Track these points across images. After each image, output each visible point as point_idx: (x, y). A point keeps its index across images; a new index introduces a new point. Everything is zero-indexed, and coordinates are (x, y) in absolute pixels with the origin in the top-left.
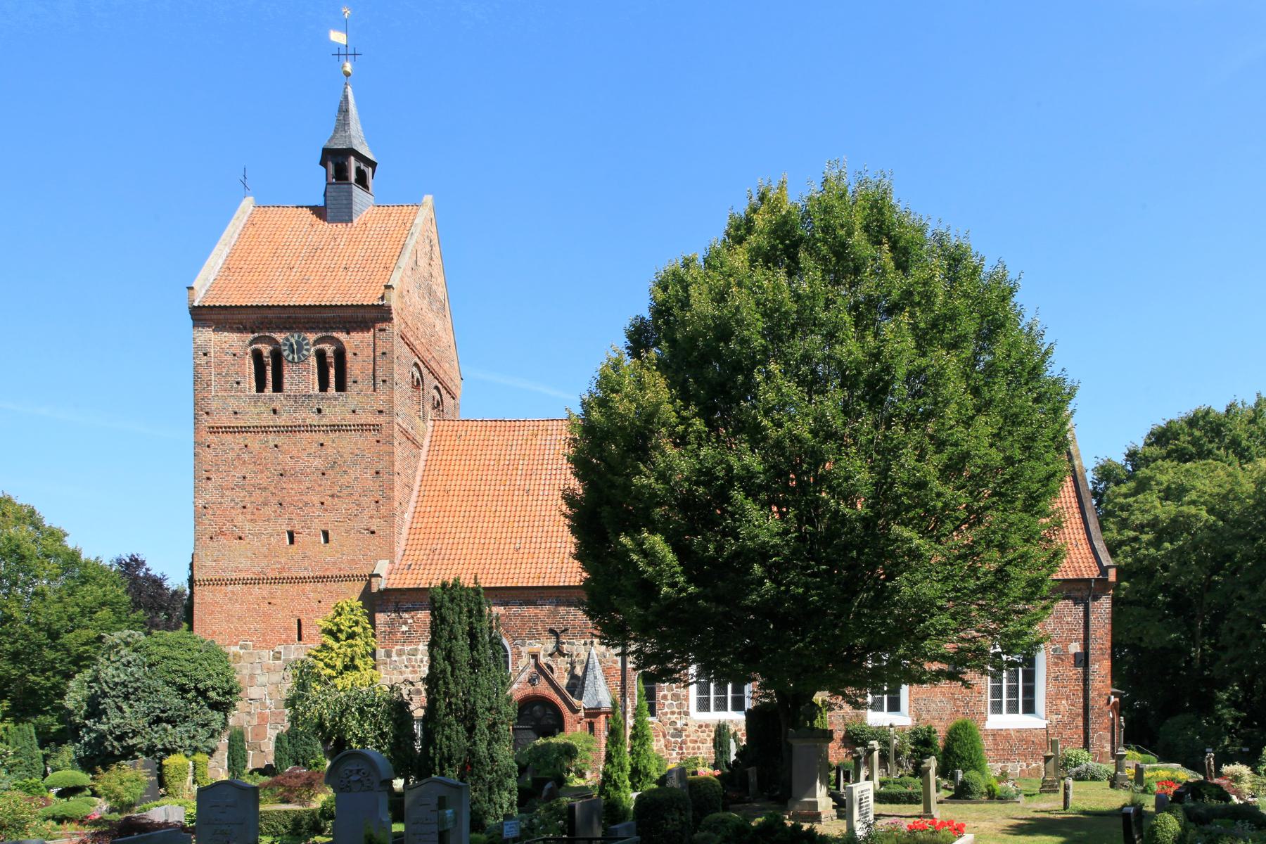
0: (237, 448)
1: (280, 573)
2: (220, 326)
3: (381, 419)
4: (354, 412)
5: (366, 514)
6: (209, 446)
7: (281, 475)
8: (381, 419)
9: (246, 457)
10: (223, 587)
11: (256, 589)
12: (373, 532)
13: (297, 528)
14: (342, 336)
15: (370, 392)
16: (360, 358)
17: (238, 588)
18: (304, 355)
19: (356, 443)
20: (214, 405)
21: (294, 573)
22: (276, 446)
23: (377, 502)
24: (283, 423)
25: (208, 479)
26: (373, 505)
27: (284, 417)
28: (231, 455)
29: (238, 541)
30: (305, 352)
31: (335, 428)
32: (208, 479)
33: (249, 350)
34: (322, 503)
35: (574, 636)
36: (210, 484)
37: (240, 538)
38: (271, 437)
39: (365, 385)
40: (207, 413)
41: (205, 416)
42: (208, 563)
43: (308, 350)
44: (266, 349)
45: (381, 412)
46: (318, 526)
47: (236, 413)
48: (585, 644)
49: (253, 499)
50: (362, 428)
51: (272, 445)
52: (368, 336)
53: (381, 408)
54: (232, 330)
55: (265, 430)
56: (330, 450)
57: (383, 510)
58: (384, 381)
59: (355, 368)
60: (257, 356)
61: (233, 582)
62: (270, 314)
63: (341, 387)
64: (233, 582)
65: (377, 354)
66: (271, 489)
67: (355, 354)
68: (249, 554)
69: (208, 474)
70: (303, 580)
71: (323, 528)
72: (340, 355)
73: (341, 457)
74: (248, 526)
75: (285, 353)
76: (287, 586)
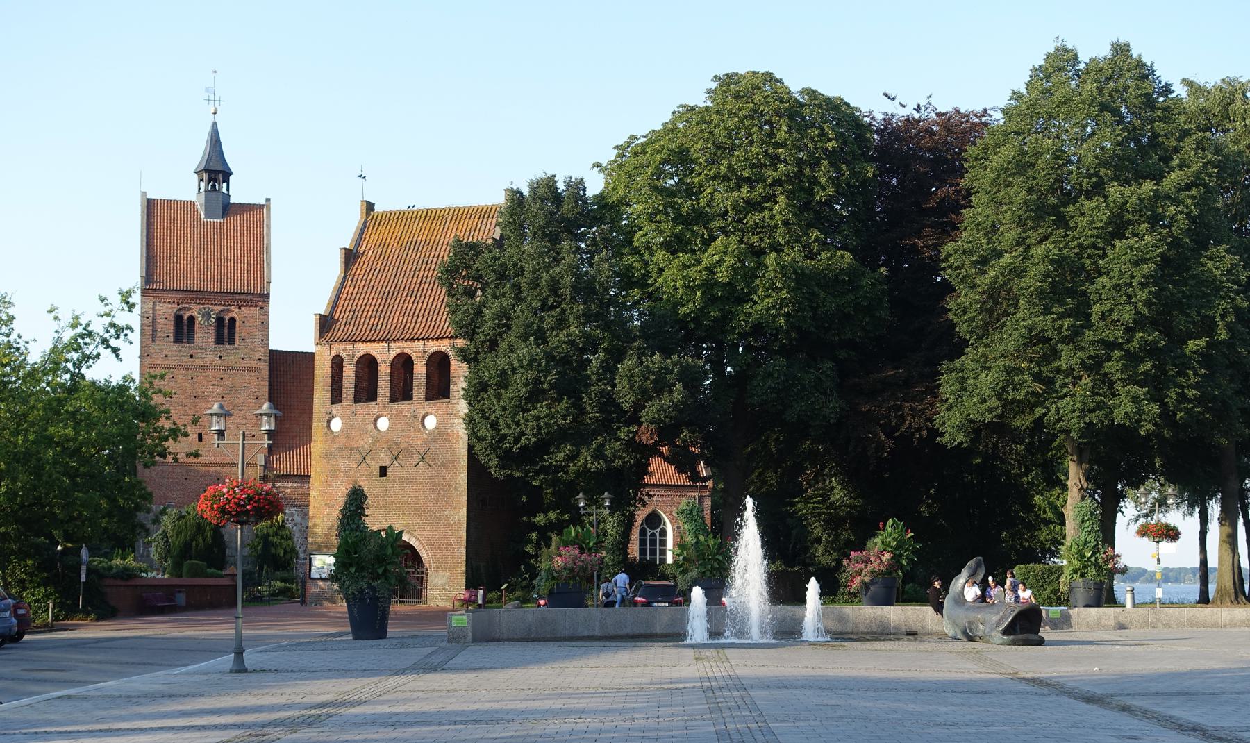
16: (247, 325)
45: (260, 359)
51: (190, 377)
55: (186, 368)
59: (240, 331)
60: (178, 319)
63: (232, 340)
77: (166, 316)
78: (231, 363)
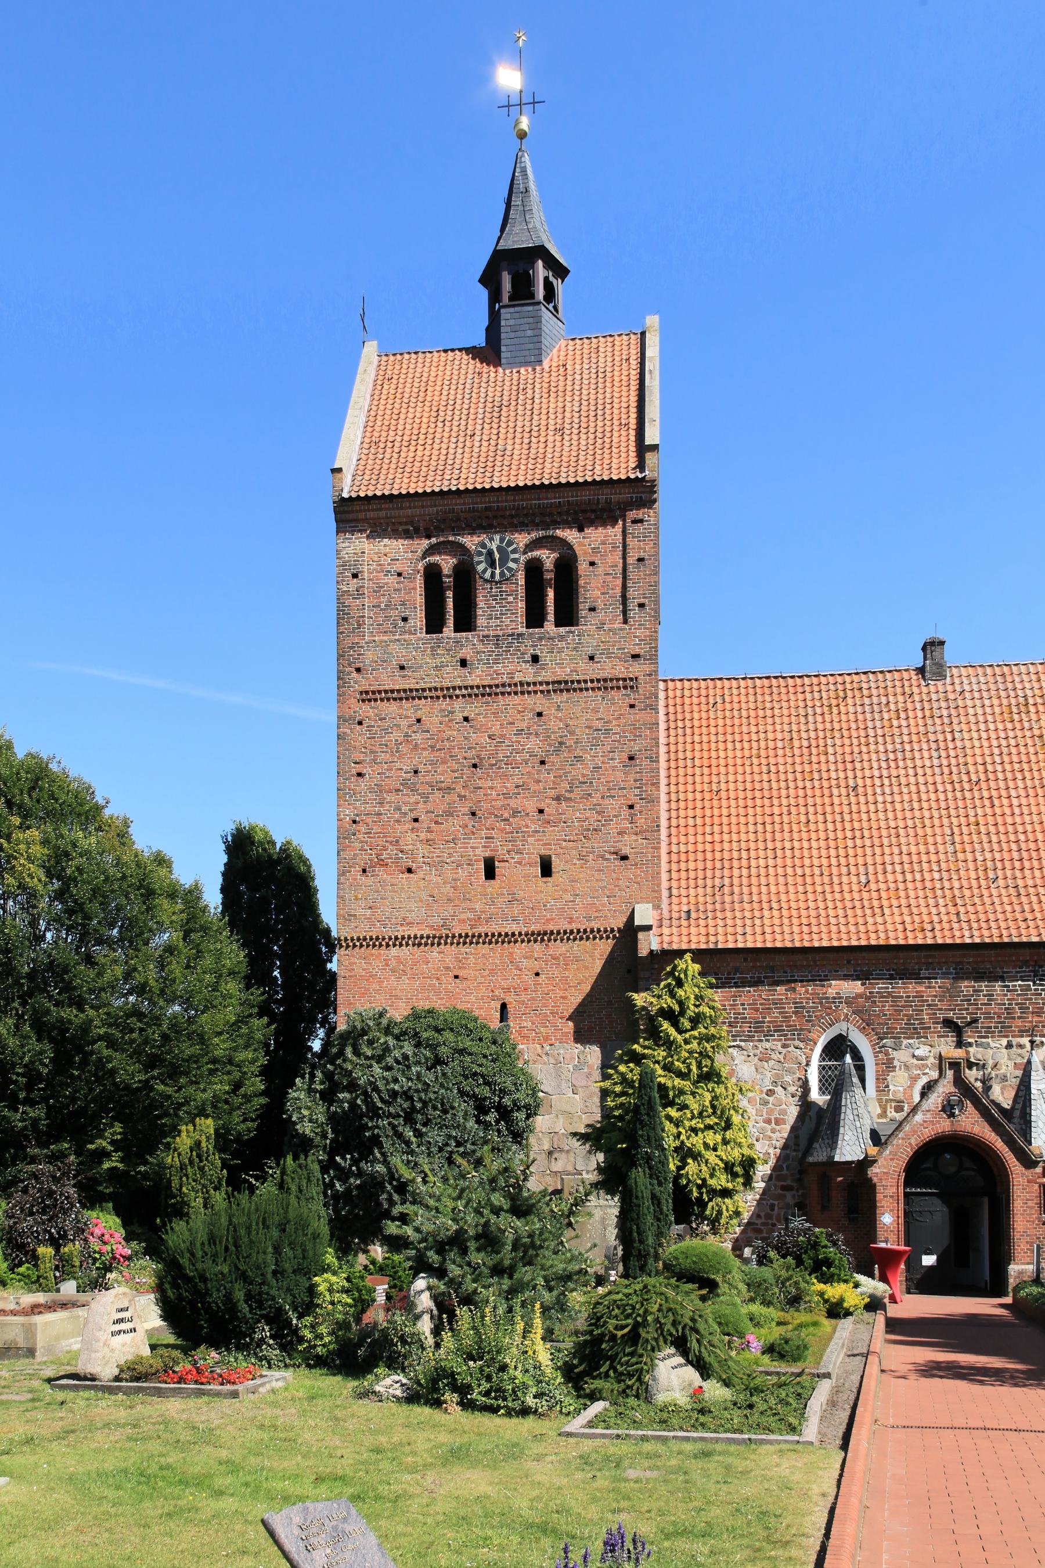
0: (404, 723)
1: (472, 927)
2: (379, 530)
3: (636, 669)
4: (592, 658)
5: (613, 827)
6: (360, 723)
7: (475, 766)
8: (636, 669)
9: (418, 737)
10: (383, 951)
11: (434, 953)
12: (624, 858)
13: (501, 852)
14: (570, 535)
15: (617, 625)
16: (600, 570)
17: (405, 952)
18: (510, 569)
19: (596, 711)
20: (369, 656)
21: (494, 928)
22: (466, 719)
23: (631, 807)
24: (477, 682)
25: (360, 775)
26: (625, 812)
27: (478, 672)
28: (396, 735)
29: (406, 875)
30: (511, 565)
31: (563, 686)
32: (360, 775)
33: (421, 566)
34: (541, 811)
35: (989, 1032)
36: (363, 784)
37: (410, 871)
38: (458, 704)
39: (610, 615)
40: (358, 670)
41: (354, 675)
42: (360, 912)
43: (515, 561)
44: (447, 563)
45: (635, 657)
46: (534, 850)
47: (402, 668)
48: (1009, 1046)
49: (430, 806)
50: (605, 684)
51: (459, 717)
52: (614, 532)
53: (637, 650)
54: (396, 534)
55: (448, 693)
56: (554, 723)
57: (641, 821)
58: (641, 606)
60: (432, 575)
61: (399, 942)
62: (458, 505)
63: (567, 616)
64: (399, 942)
65: (630, 561)
66: (459, 789)
67: (592, 564)
68: (424, 896)
69: (359, 768)
70: (510, 938)
71: (543, 852)
72: (567, 567)
73: (572, 733)
74: (422, 850)
75: (480, 568)
76: (484, 949)
77: (398, 567)
78: (562, 674)
